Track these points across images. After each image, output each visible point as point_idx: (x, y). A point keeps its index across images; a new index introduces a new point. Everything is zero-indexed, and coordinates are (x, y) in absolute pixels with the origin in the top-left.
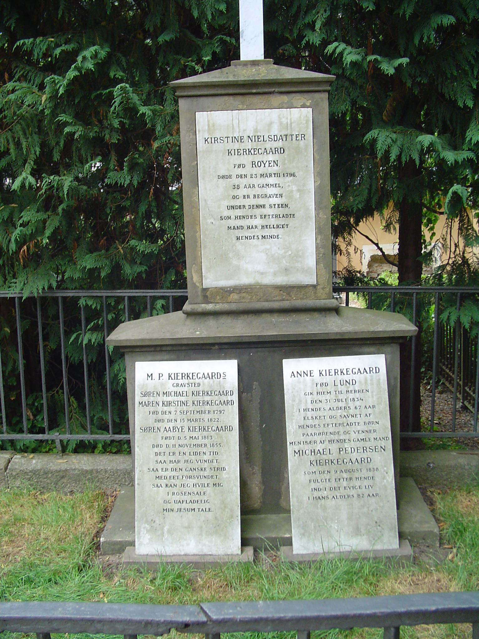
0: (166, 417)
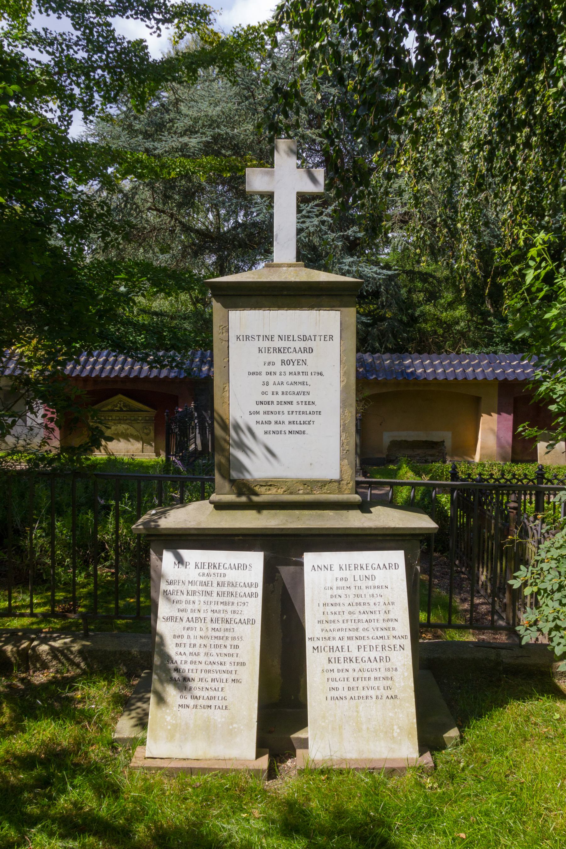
0: (190, 607)
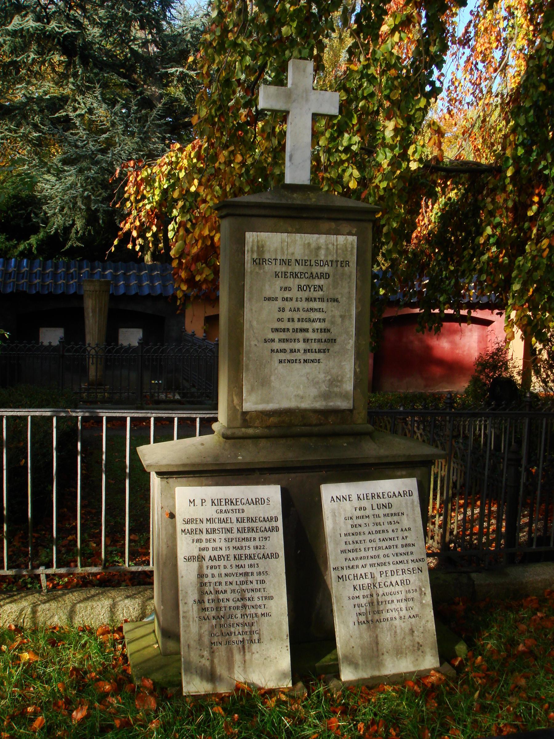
0: (210, 545)
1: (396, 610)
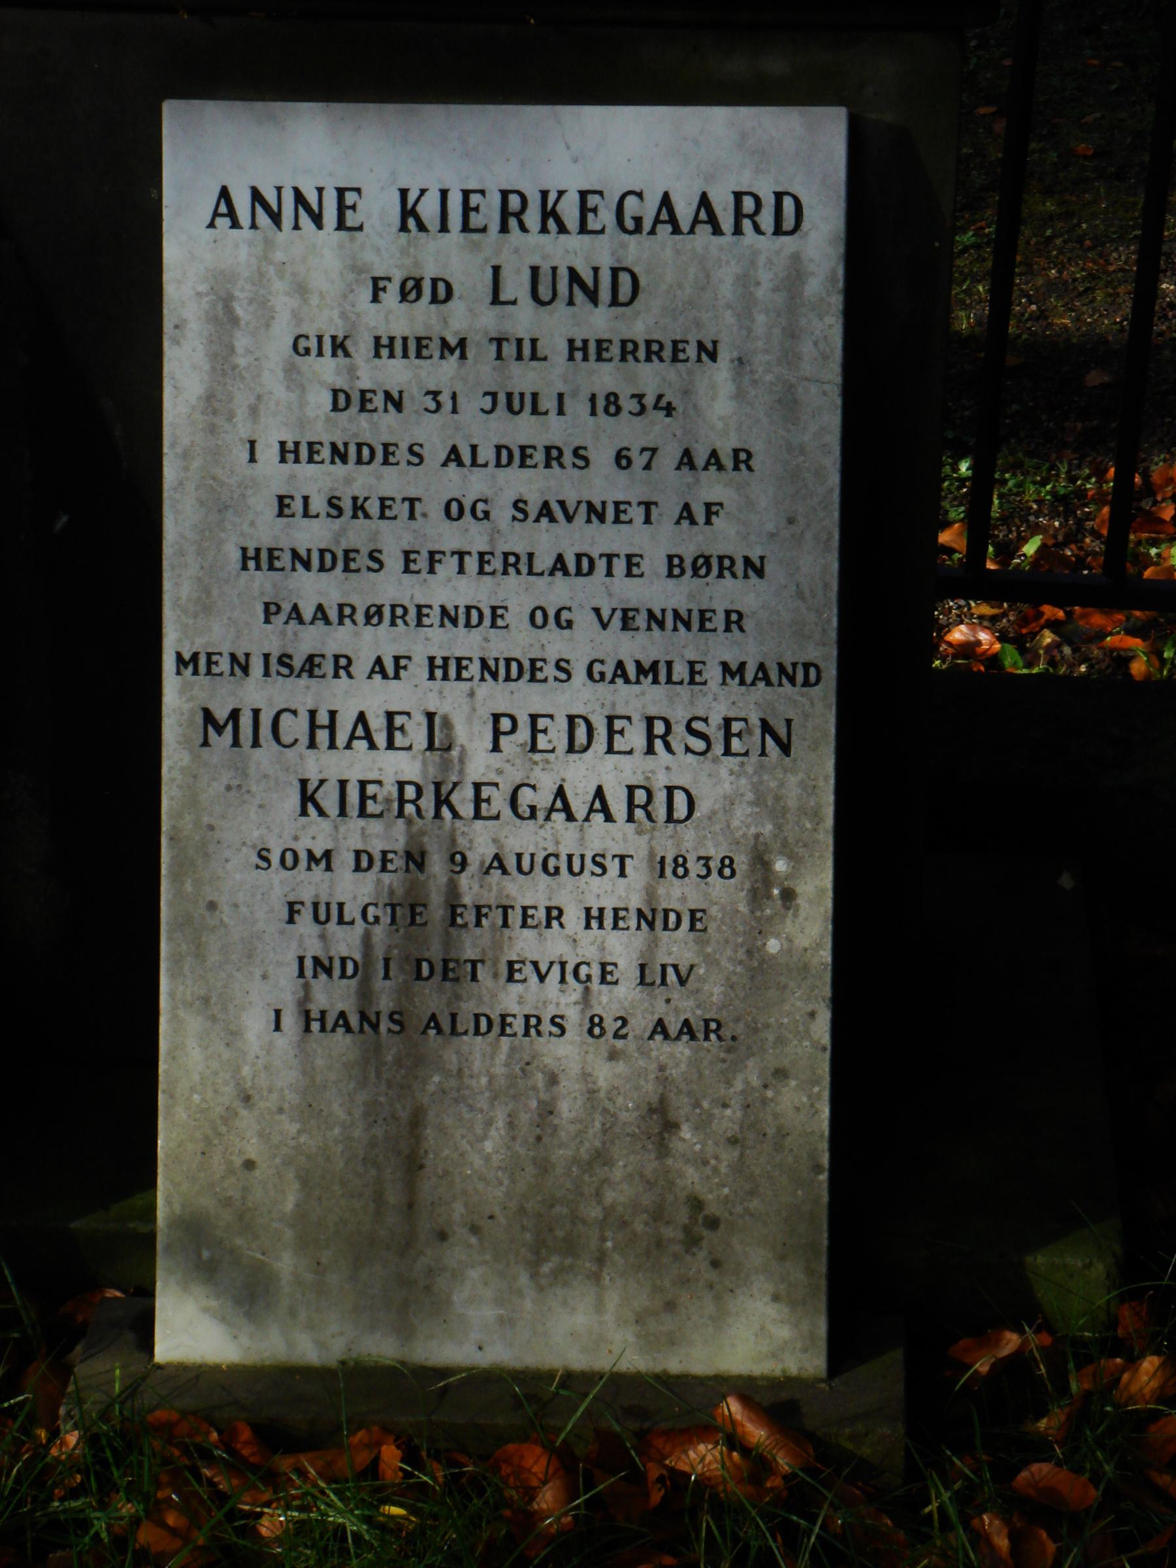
1: (570, 972)
